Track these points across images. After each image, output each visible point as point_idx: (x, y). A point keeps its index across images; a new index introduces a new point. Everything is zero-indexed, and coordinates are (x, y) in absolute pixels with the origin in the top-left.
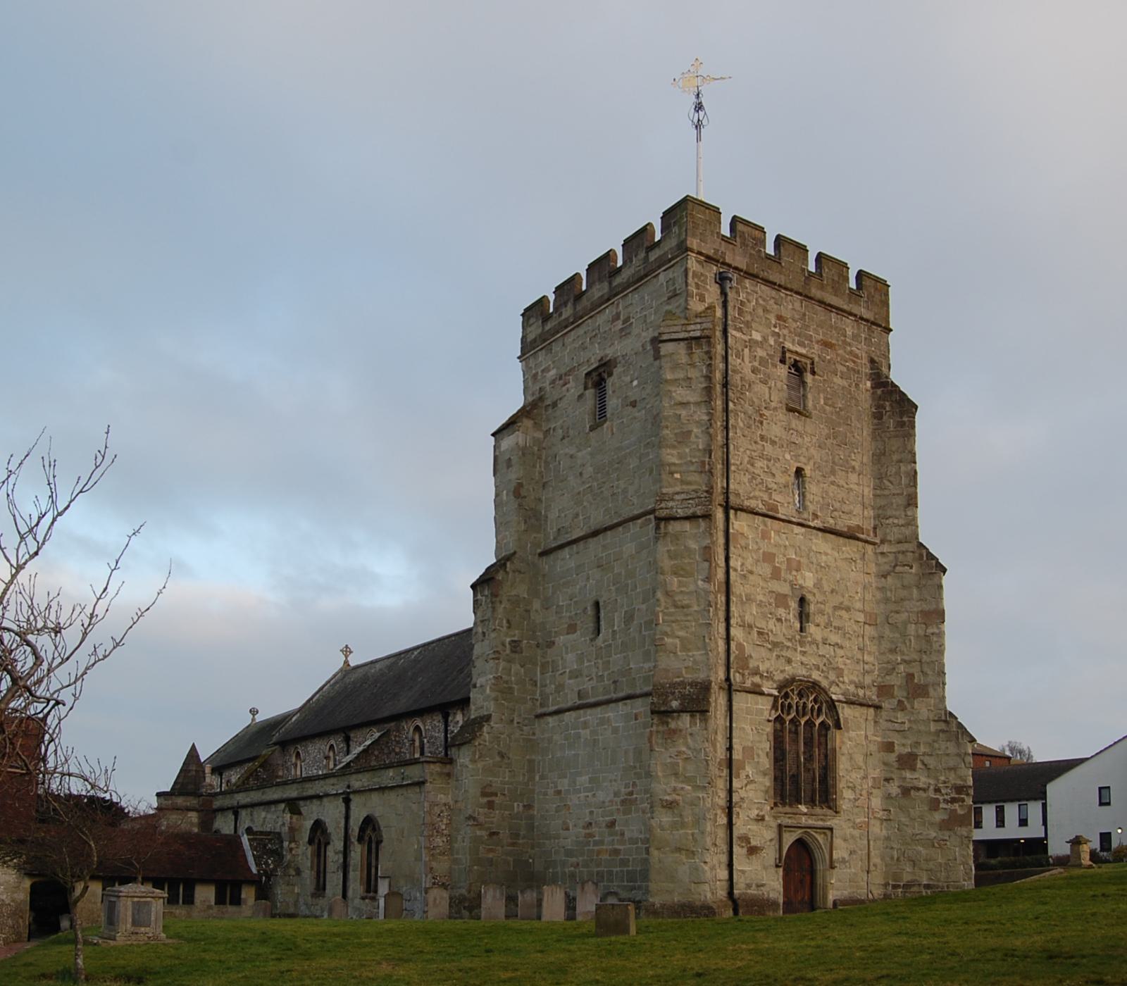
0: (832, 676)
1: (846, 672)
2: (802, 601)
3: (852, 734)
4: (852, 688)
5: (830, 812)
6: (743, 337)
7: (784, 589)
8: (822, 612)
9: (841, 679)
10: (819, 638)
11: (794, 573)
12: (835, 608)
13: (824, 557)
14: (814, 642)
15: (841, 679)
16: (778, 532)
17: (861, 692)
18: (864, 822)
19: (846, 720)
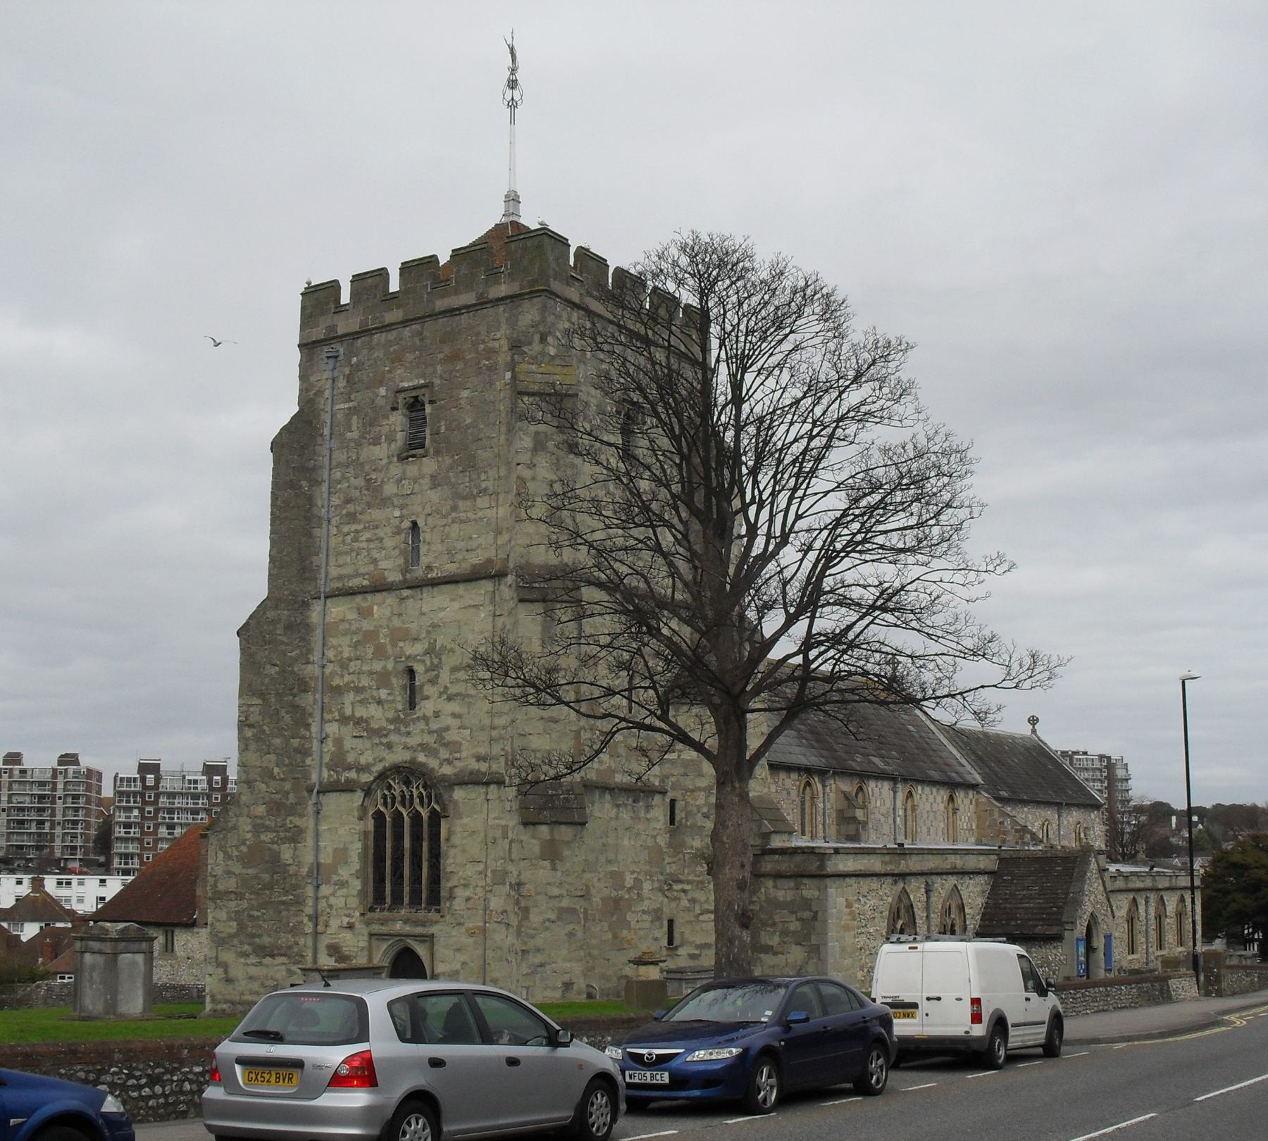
0: (444, 754)
1: (465, 745)
2: (411, 672)
3: (466, 820)
4: (475, 765)
5: (437, 916)
6: (351, 404)
7: (390, 665)
8: (433, 681)
9: (457, 755)
10: (429, 713)
11: (401, 644)
12: (454, 669)
13: (441, 615)
14: (425, 718)
15: (457, 755)
16: (380, 605)
17: (483, 767)
18: (477, 928)
19: (456, 803)
